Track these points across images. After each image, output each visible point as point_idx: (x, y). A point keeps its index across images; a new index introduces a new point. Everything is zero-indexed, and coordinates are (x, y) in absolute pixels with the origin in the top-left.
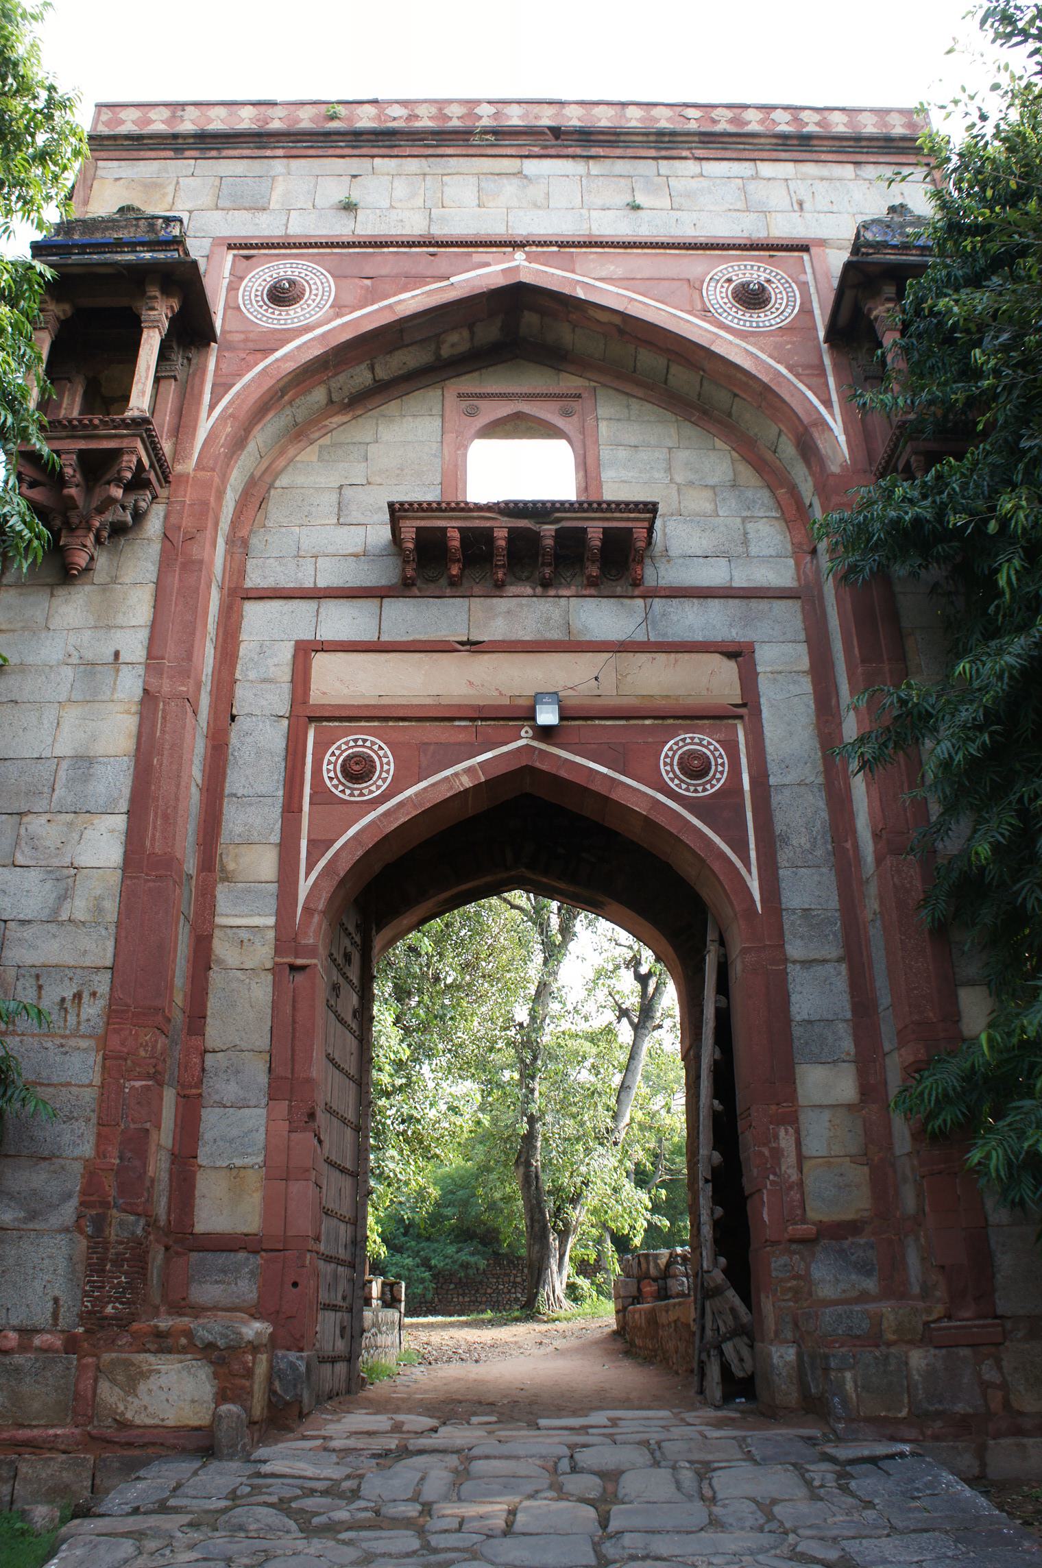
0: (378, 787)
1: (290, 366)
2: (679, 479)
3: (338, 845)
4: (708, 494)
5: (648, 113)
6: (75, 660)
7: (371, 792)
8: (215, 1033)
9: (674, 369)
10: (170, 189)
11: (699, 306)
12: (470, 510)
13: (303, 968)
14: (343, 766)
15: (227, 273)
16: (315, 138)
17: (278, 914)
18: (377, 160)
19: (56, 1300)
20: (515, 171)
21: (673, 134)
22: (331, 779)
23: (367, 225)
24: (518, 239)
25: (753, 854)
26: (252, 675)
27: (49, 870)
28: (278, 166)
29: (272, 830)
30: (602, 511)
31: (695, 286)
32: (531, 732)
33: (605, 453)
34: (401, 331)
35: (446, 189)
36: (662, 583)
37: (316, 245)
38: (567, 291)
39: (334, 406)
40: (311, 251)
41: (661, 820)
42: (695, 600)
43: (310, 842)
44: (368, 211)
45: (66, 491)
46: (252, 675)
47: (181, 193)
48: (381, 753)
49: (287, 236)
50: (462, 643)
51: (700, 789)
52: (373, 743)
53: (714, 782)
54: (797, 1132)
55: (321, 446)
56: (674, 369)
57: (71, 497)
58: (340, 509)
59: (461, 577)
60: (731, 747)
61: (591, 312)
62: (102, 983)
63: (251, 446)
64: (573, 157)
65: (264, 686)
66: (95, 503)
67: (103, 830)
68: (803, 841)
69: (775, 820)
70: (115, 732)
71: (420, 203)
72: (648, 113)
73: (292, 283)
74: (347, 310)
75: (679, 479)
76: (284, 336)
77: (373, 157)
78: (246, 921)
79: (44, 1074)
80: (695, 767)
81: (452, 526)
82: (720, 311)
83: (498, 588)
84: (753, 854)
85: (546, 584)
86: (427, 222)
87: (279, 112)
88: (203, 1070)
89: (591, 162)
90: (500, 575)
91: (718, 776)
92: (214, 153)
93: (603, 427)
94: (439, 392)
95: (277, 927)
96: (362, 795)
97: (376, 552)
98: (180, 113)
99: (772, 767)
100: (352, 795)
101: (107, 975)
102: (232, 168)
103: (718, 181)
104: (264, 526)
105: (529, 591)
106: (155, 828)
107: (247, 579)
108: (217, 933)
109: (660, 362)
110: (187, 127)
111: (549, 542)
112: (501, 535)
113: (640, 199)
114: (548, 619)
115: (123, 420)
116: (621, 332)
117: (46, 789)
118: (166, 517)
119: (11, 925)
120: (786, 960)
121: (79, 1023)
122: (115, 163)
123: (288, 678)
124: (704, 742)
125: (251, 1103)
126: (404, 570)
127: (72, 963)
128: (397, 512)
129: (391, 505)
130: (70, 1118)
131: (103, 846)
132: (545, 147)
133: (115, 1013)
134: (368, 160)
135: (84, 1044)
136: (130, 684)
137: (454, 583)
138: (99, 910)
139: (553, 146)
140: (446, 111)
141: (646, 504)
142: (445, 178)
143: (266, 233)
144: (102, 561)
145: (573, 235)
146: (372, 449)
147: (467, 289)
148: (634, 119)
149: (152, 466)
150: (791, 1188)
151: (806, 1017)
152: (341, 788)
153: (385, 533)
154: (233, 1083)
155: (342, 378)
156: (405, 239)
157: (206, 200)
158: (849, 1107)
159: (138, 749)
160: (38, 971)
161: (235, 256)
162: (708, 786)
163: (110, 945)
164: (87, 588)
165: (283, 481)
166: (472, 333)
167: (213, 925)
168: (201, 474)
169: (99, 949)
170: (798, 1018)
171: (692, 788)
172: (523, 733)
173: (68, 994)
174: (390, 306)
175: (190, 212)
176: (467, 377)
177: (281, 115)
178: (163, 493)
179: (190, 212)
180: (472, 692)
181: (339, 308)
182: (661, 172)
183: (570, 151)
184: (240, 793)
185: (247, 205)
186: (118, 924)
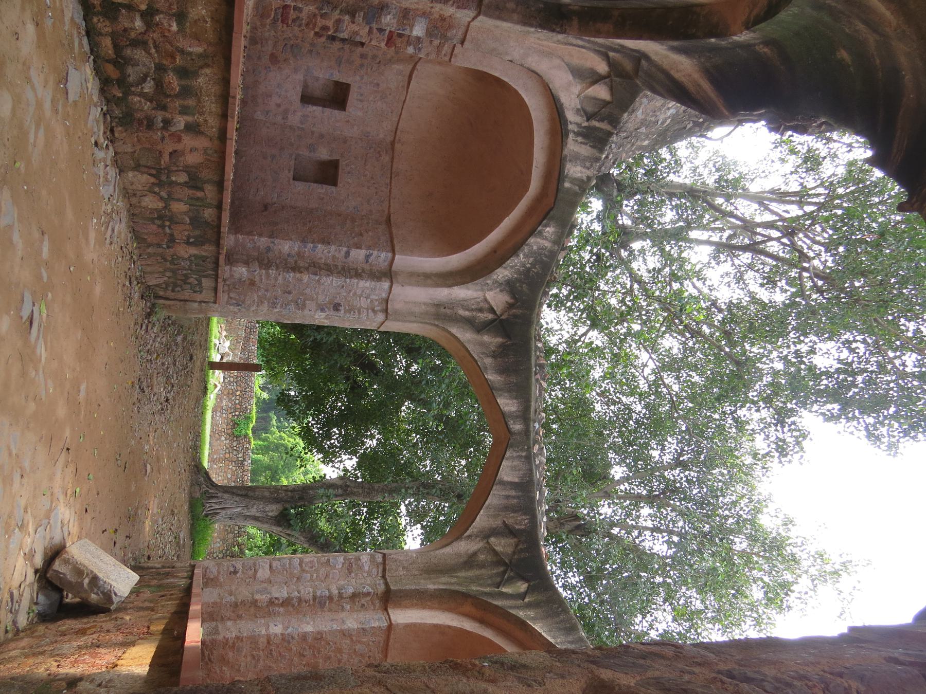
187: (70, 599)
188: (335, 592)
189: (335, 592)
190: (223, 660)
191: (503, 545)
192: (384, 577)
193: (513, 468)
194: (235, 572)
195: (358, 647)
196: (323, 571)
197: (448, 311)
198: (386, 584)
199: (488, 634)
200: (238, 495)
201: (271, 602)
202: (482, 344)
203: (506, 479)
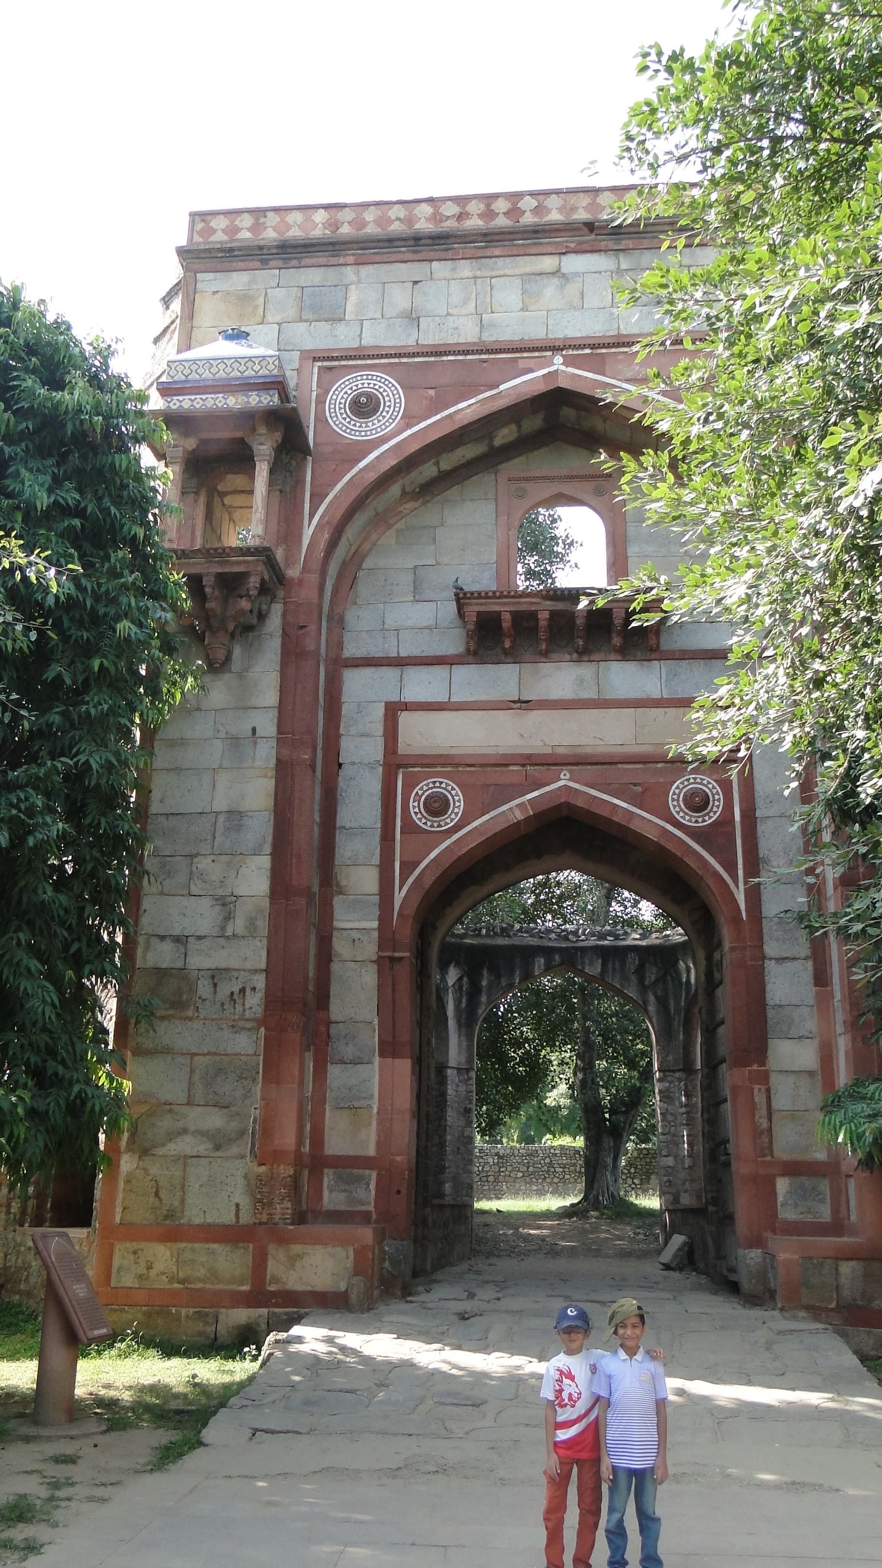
0: (452, 820)
1: (372, 476)
3: (423, 865)
6: (222, 735)
7: (447, 824)
8: (337, 1010)
10: (261, 300)
13: (401, 959)
14: (425, 804)
15: (314, 387)
16: (380, 244)
17: (381, 919)
18: (434, 263)
19: (237, 1205)
20: (555, 269)
22: (416, 813)
23: (431, 336)
24: (556, 344)
28: (349, 273)
34: (461, 435)
35: (495, 292)
37: (387, 356)
40: (383, 361)
41: (669, 846)
42: (702, 662)
44: (429, 319)
45: (208, 605)
46: (353, 731)
47: (270, 306)
48: (453, 792)
51: (700, 820)
52: (447, 785)
53: (711, 814)
54: (768, 1090)
55: (397, 531)
57: (212, 610)
58: (415, 588)
59: (513, 647)
60: (726, 785)
62: (260, 981)
63: (343, 542)
65: (364, 739)
66: (231, 612)
69: (760, 846)
70: (257, 792)
71: (471, 306)
73: (370, 396)
78: (356, 924)
80: (698, 803)
81: (505, 609)
84: (740, 873)
86: (478, 329)
87: (347, 215)
88: (329, 1036)
89: (621, 255)
90: (543, 646)
91: (715, 809)
92: (294, 263)
94: (493, 477)
95: (380, 928)
96: (439, 826)
98: (262, 220)
99: (760, 802)
100: (432, 826)
102: (311, 276)
104: (356, 603)
105: (567, 657)
107: (345, 650)
108: (335, 933)
110: (270, 235)
112: (543, 616)
114: (582, 681)
115: (248, 549)
117: (209, 837)
118: (284, 615)
119: (190, 939)
120: (763, 958)
121: (244, 1010)
122: (210, 276)
123: (380, 732)
125: (366, 1060)
126: (468, 643)
128: (462, 598)
130: (241, 1078)
131: (254, 880)
134: (426, 265)
135: (249, 1025)
136: (266, 754)
138: (251, 925)
140: (493, 207)
142: (493, 280)
143: (345, 345)
144: (237, 651)
149: (271, 578)
151: (778, 1003)
152: (424, 821)
153: (453, 607)
155: (413, 475)
156: (461, 348)
157: (291, 312)
158: (811, 1074)
159: (275, 805)
162: (707, 818)
163: (264, 954)
164: (227, 676)
165: (368, 563)
166: (519, 427)
167: (332, 929)
171: (693, 820)
172: (562, 776)
173: (236, 990)
174: (450, 416)
175: (279, 324)
177: (350, 219)
178: (281, 593)
179: (279, 324)
181: (409, 419)
184: (348, 826)
185: (326, 316)
186: (269, 938)
187: (685, 1262)
188: (684, 1110)
189: (684, 1110)
191: (651, 976)
192: (673, 1071)
193: (591, 964)
194: (669, 1181)
196: (670, 1118)
197: (464, 1016)
198: (679, 1071)
202: (490, 986)
203: (599, 970)
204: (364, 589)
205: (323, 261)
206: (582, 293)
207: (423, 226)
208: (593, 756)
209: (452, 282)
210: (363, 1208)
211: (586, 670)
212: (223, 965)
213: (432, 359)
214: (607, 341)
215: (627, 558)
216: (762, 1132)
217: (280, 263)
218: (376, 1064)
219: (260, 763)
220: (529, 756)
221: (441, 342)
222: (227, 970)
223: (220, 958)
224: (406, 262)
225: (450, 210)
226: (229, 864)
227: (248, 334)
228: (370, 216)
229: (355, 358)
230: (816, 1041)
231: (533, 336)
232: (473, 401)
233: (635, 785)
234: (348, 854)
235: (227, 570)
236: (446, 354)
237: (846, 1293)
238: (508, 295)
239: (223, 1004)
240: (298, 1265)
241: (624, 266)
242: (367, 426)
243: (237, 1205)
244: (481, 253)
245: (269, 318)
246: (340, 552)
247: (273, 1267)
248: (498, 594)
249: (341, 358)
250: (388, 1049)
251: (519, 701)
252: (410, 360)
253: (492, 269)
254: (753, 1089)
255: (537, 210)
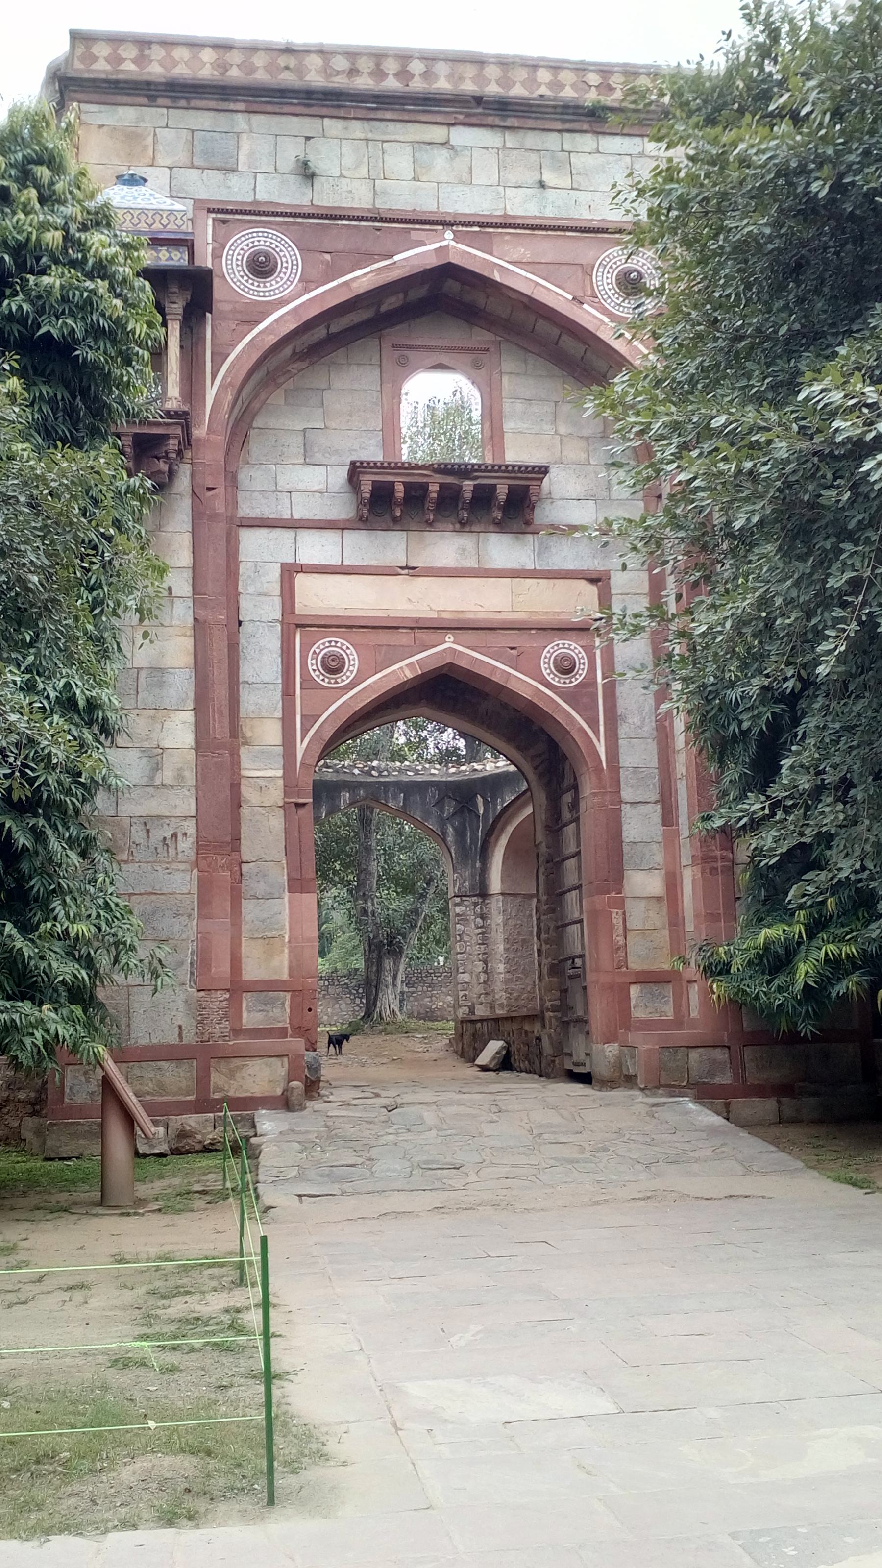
0: (348, 677)
1: (272, 339)
2: (563, 430)
4: (583, 444)
5: (555, 76)
7: (343, 681)
8: (247, 851)
9: (565, 337)
10: (150, 139)
11: (589, 293)
12: (413, 468)
13: (304, 805)
14: (322, 662)
15: (210, 240)
18: (326, 120)
19: (180, 1027)
20: (444, 141)
21: (577, 107)
23: (326, 196)
24: (448, 219)
25: (602, 728)
26: (251, 590)
27: (143, 750)
28: (241, 121)
29: (276, 708)
30: (508, 472)
31: (587, 270)
32: (452, 639)
33: (507, 406)
35: (386, 157)
36: (546, 521)
37: (282, 214)
38: (486, 274)
39: (298, 356)
43: (302, 716)
47: (160, 147)
48: (348, 652)
49: (256, 202)
50: (402, 568)
52: (343, 644)
54: (624, 913)
56: (565, 337)
60: (590, 651)
61: (504, 290)
62: (190, 827)
64: (492, 127)
67: (178, 722)
68: (635, 720)
71: (363, 171)
72: (555, 76)
73: (267, 255)
74: (313, 286)
75: (563, 430)
76: (264, 309)
77: (322, 117)
79: (157, 887)
82: (605, 297)
83: (430, 525)
84: (602, 728)
85: (463, 524)
86: (371, 195)
89: (507, 133)
92: (183, 103)
93: (505, 380)
95: (284, 777)
96: (336, 683)
97: (336, 489)
101: (194, 821)
103: (611, 158)
105: (451, 527)
106: (214, 720)
108: (243, 781)
109: (556, 332)
111: (468, 495)
112: (434, 488)
113: (549, 177)
114: (464, 550)
116: (526, 307)
118: (192, 475)
123: (278, 592)
124: (572, 648)
125: (276, 895)
126: (358, 509)
127: (168, 814)
129: (353, 463)
130: (176, 915)
131: (179, 732)
132: (468, 115)
133: (201, 846)
134: (318, 121)
135: (182, 867)
137: (395, 520)
138: (180, 777)
139: (475, 115)
141: (540, 467)
142: (385, 144)
145: (490, 216)
146: (327, 395)
147: (408, 269)
148: (542, 87)
150: (619, 948)
153: (343, 473)
154: (262, 883)
155: (305, 337)
157: (182, 157)
158: (659, 899)
160: (145, 820)
161: (214, 219)
165: (258, 422)
166: (406, 295)
167: (240, 777)
168: (212, 437)
169: (184, 803)
170: (627, 840)
173: (168, 835)
174: (346, 283)
175: (171, 168)
176: (398, 327)
178: (188, 454)
179: (171, 168)
180: (410, 607)
181: (307, 283)
182: (566, 147)
183: (490, 120)
185: (219, 164)
190: (517, 999)
191: (449, 808)
193: (395, 797)
194: (465, 995)
195: (513, 914)
199: (510, 829)
200: (377, 994)
201: (485, 972)
204: (256, 447)
205: (212, 104)
206: (471, 168)
207: (315, 79)
208: (474, 621)
209: (344, 142)
210: (280, 1025)
211: (466, 541)
212: (154, 813)
213: (327, 222)
214: (494, 221)
215: (503, 432)
216: (619, 948)
217: (167, 102)
218: (286, 899)
219: (178, 623)
220: (417, 620)
221: (336, 205)
222: (159, 817)
223: (152, 806)
224: (297, 115)
225: (340, 63)
226: (153, 718)
227: (145, 180)
228: (259, 60)
229: (250, 213)
230: (663, 872)
231: (425, 209)
232: (368, 269)
233: (512, 648)
234: (252, 708)
235: (146, 430)
236: (341, 218)
237: (694, 1073)
238: (399, 161)
239: (156, 848)
240: (238, 1075)
241: (509, 145)
242: (265, 286)
243: (180, 1027)
244: (372, 115)
245: (160, 161)
246: (236, 411)
247: (216, 1078)
248: (393, 465)
249: (236, 212)
250: (296, 885)
251: (407, 567)
252: (305, 221)
253: (384, 133)
254: (611, 913)
255: (427, 75)
